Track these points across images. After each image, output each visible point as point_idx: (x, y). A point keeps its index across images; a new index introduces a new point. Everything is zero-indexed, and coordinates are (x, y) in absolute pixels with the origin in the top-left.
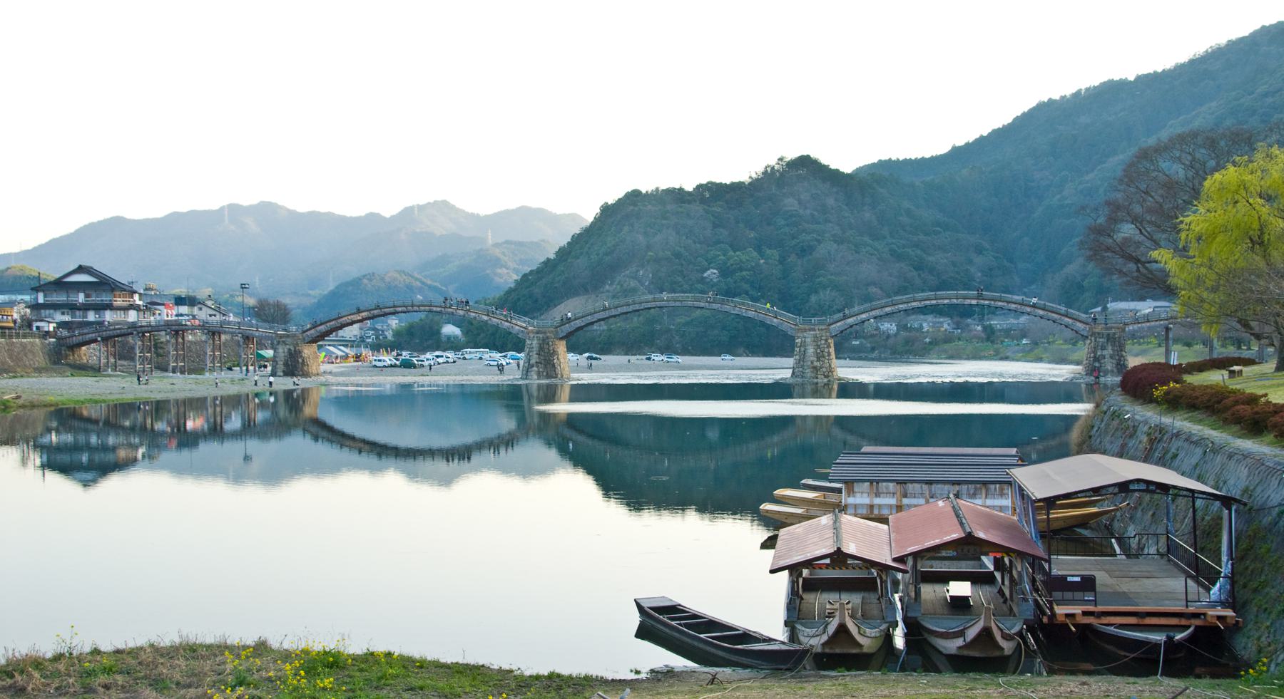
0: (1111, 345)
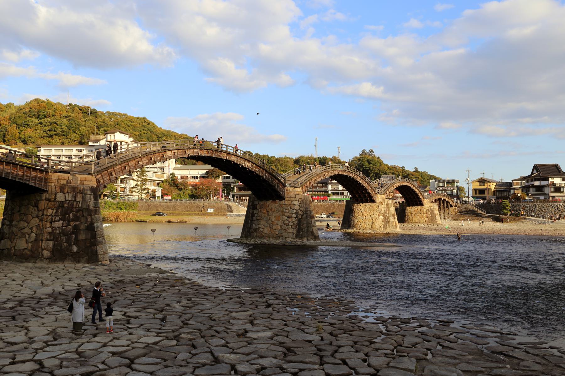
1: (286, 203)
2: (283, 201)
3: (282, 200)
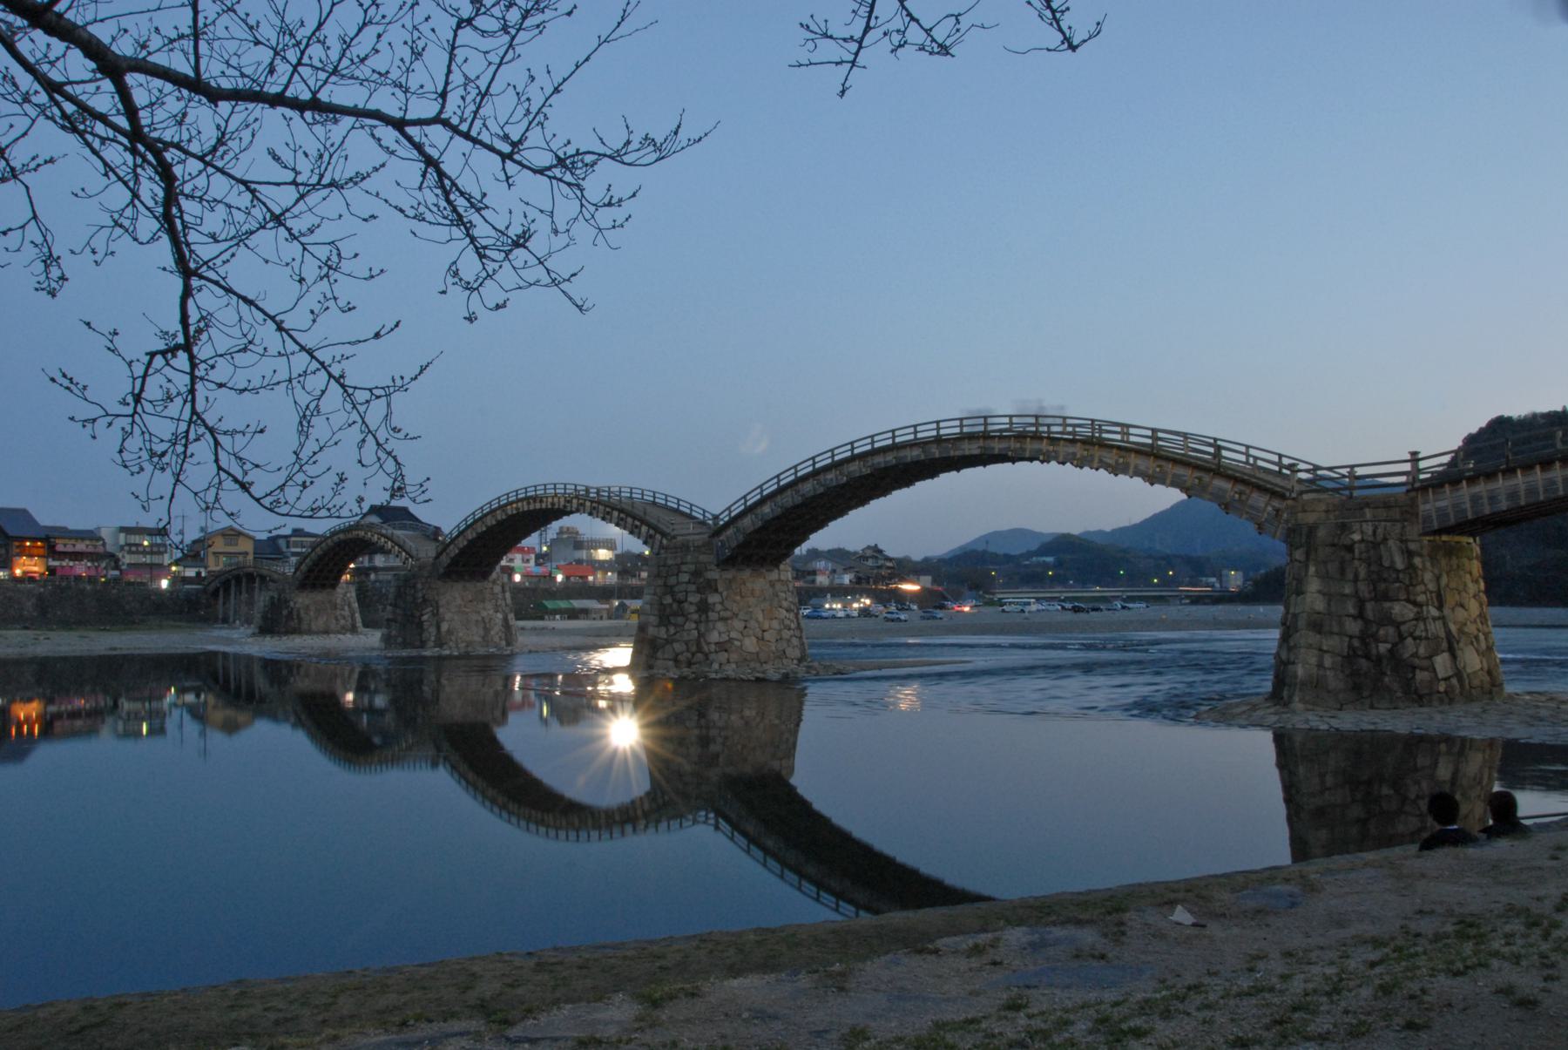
0: (1324, 577)
1: (782, 578)
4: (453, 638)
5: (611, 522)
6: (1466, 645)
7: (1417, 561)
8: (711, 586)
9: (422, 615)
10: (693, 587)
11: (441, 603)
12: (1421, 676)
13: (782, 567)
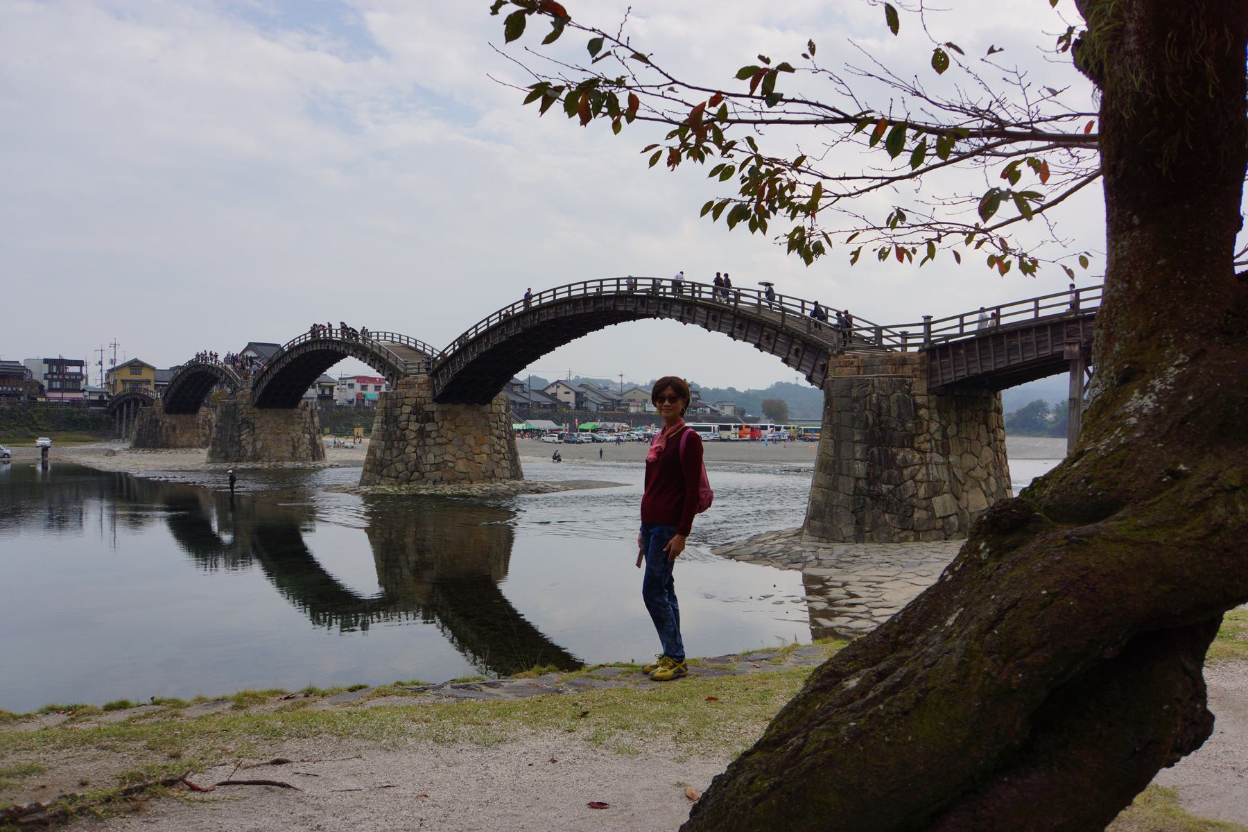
2: (489, 405)
3: (485, 404)
4: (266, 454)
5: (365, 362)
6: (972, 487)
7: (923, 412)
8: (428, 418)
9: (241, 435)
10: (413, 417)
11: (256, 426)
12: (919, 515)
13: (494, 401)
